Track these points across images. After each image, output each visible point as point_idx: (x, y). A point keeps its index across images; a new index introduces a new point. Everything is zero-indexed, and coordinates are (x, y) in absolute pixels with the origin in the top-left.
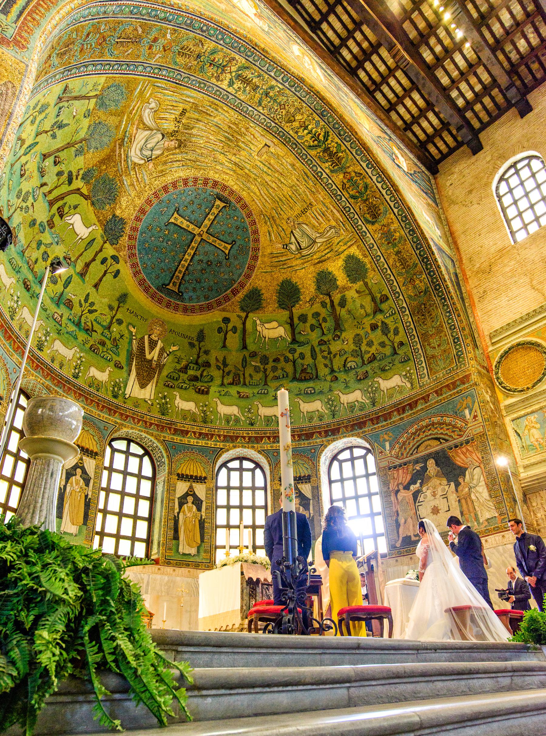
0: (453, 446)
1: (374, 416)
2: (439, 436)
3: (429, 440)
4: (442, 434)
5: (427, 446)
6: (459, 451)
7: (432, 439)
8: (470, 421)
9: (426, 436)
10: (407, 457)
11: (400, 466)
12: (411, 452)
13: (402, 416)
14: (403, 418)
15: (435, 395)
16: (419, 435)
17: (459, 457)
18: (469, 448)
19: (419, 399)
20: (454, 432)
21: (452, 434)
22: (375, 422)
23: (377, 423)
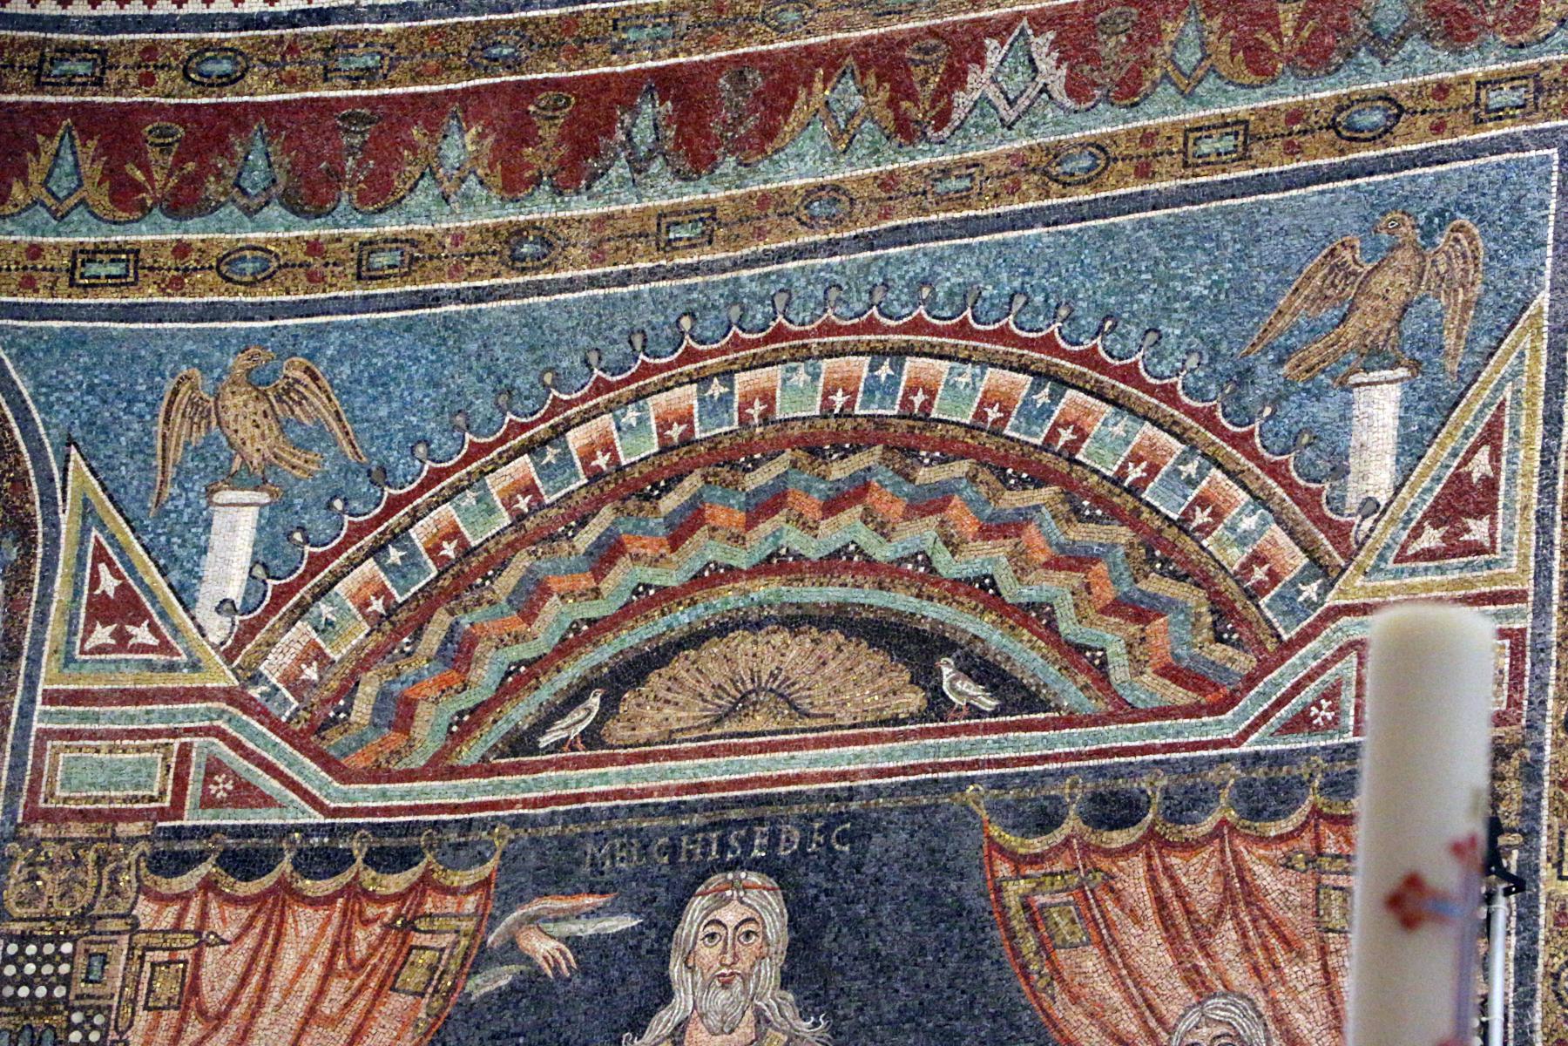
0: (1073, 795)
1: (169, 92)
2: (934, 612)
3: (796, 620)
4: (983, 591)
5: (743, 703)
6: (1133, 878)
7: (837, 619)
8: (1387, 533)
9: (775, 565)
10: (441, 768)
11: (327, 861)
12: (520, 713)
13: (541, 209)
14: (549, 241)
15: (1053, 73)
16: (680, 531)
17: (1108, 946)
18: (1265, 877)
19: (830, 61)
20: (1139, 611)
21: (1112, 638)
22: (160, 176)
23: (183, 204)
